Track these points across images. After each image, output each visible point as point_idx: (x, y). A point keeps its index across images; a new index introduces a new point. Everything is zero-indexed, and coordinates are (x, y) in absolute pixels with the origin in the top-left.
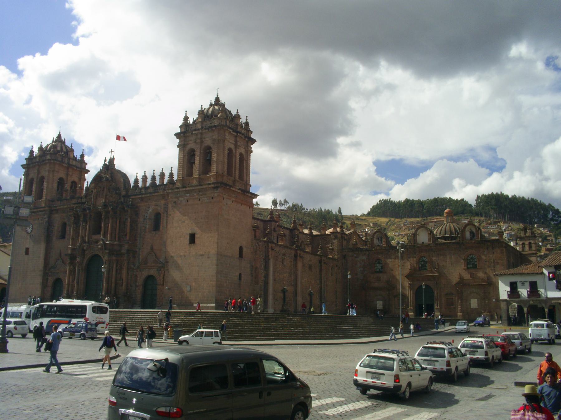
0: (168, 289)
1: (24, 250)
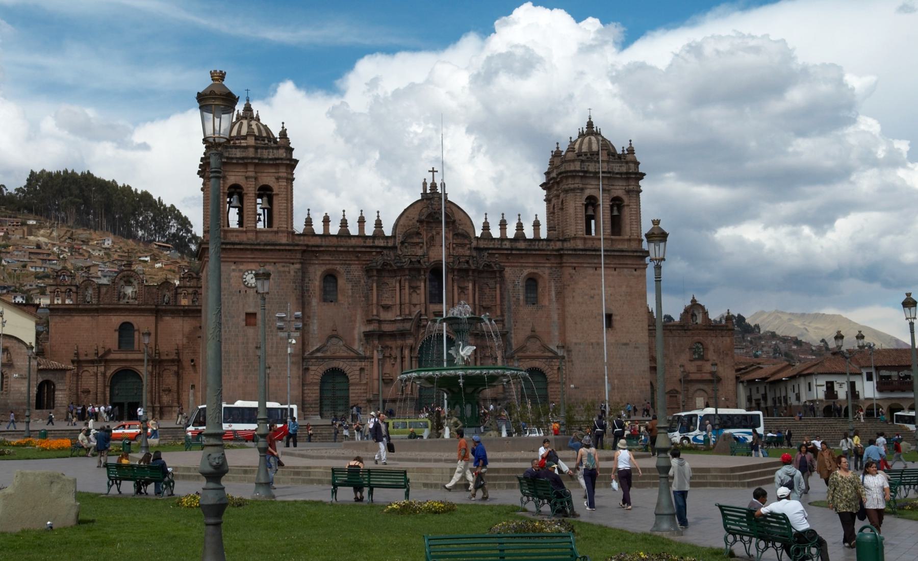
0: (575, 388)
1: (243, 316)
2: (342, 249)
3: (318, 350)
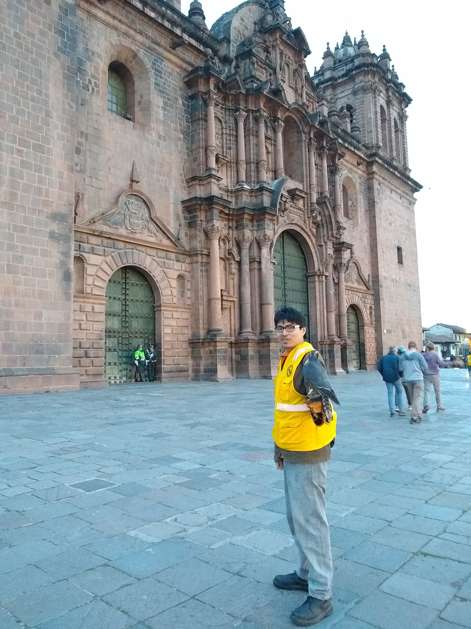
2: (152, 15)
3: (104, 217)
